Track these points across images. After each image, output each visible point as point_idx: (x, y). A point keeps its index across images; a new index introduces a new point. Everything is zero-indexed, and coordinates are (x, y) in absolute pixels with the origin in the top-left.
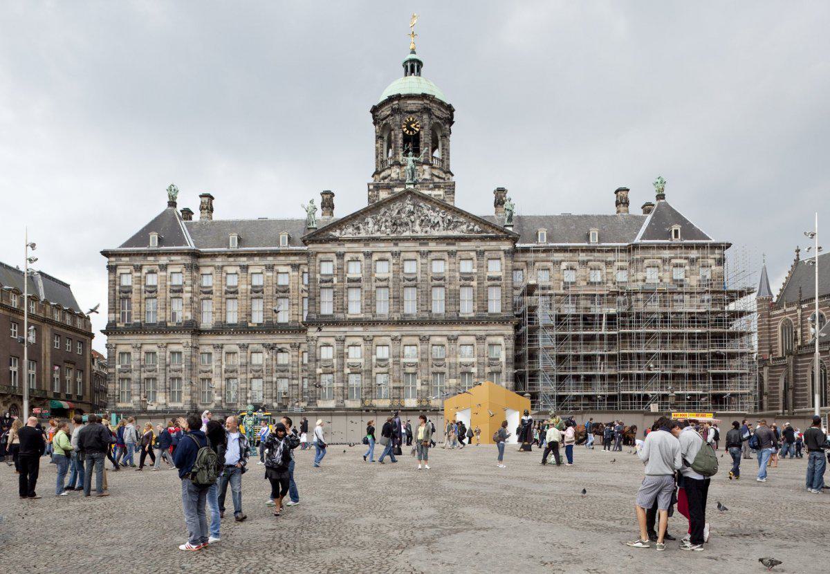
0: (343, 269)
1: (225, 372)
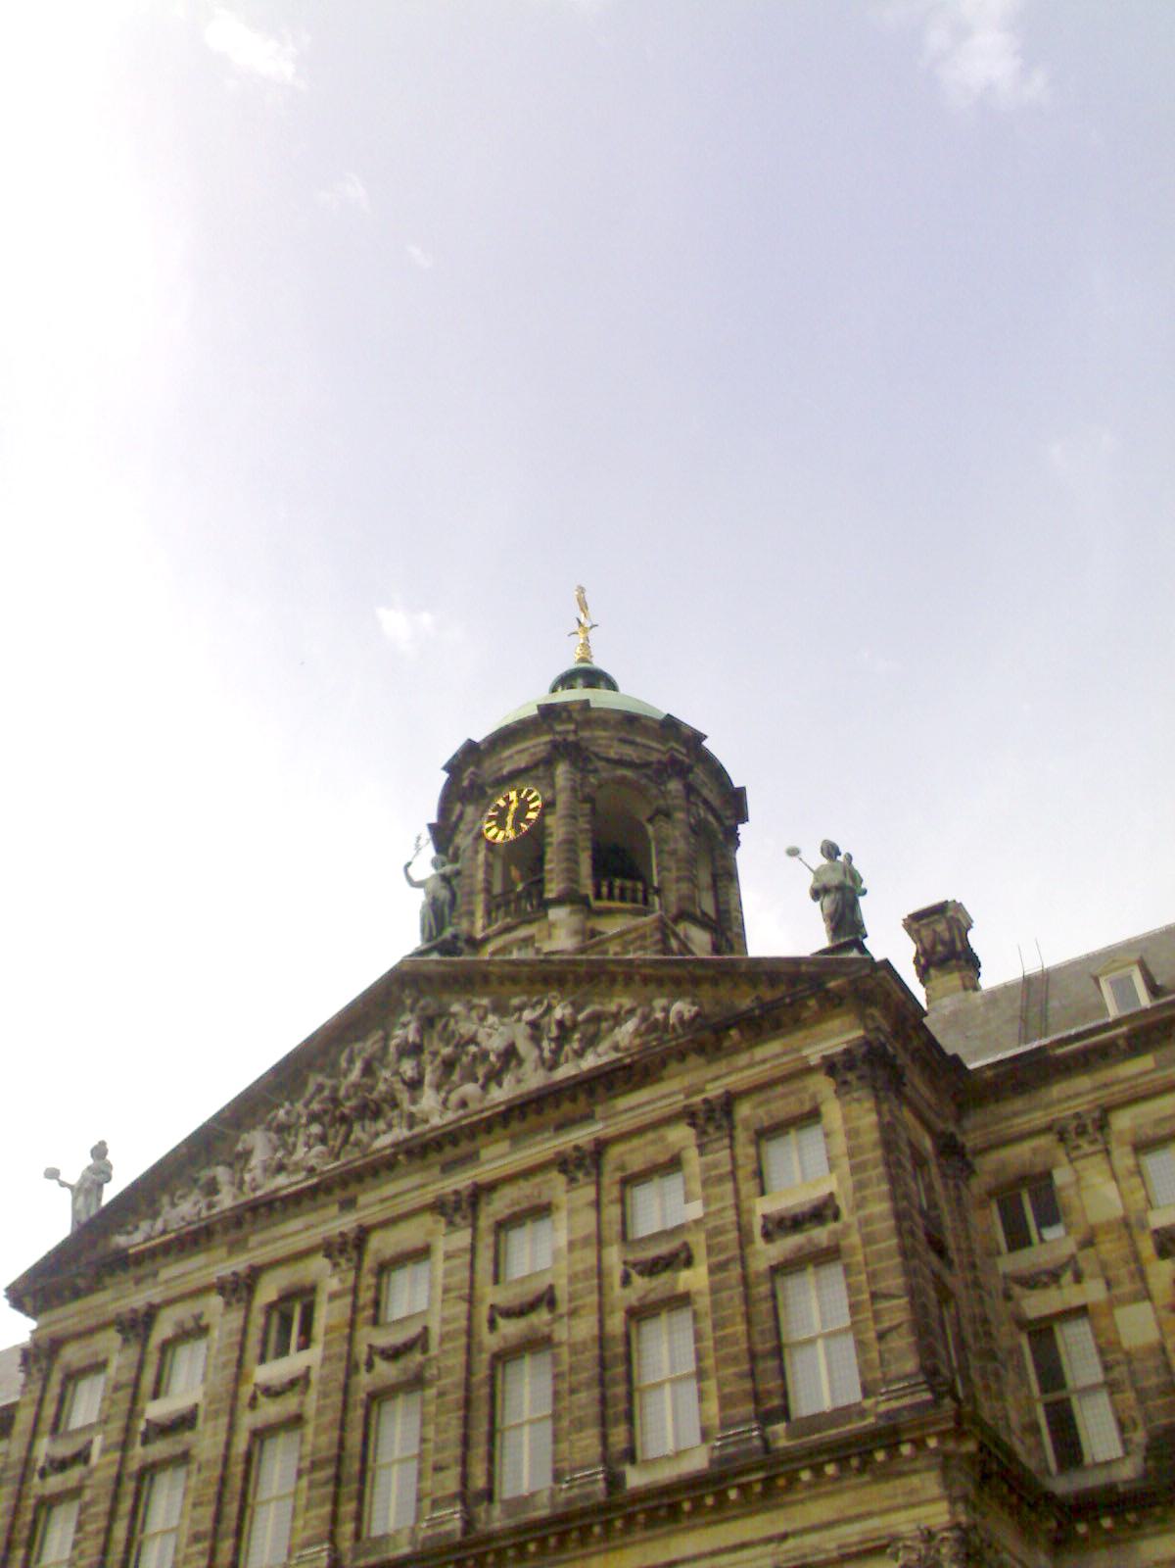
0: (136, 1383)
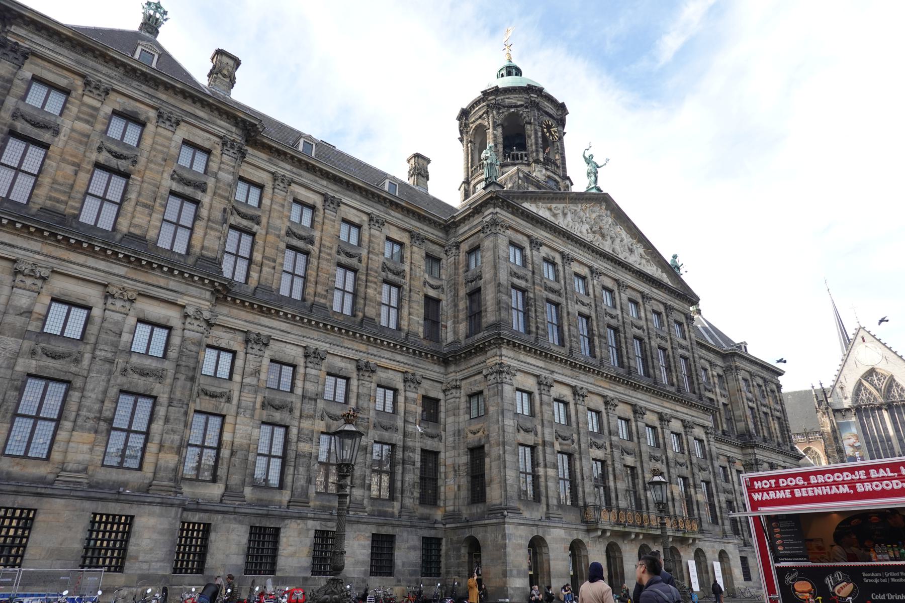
1: (263, 406)
